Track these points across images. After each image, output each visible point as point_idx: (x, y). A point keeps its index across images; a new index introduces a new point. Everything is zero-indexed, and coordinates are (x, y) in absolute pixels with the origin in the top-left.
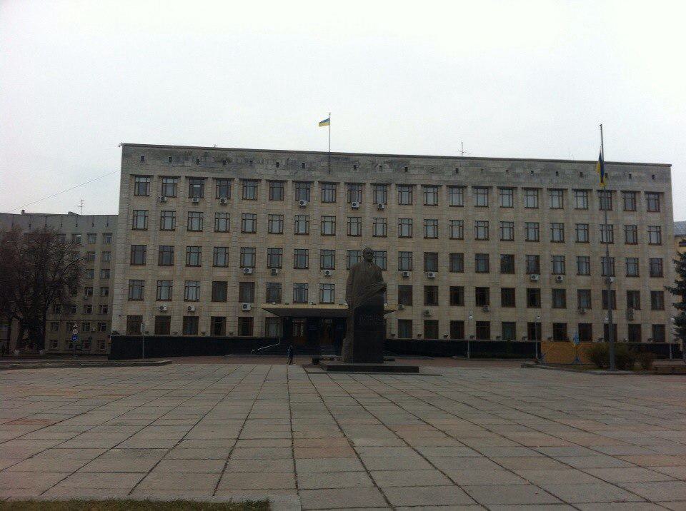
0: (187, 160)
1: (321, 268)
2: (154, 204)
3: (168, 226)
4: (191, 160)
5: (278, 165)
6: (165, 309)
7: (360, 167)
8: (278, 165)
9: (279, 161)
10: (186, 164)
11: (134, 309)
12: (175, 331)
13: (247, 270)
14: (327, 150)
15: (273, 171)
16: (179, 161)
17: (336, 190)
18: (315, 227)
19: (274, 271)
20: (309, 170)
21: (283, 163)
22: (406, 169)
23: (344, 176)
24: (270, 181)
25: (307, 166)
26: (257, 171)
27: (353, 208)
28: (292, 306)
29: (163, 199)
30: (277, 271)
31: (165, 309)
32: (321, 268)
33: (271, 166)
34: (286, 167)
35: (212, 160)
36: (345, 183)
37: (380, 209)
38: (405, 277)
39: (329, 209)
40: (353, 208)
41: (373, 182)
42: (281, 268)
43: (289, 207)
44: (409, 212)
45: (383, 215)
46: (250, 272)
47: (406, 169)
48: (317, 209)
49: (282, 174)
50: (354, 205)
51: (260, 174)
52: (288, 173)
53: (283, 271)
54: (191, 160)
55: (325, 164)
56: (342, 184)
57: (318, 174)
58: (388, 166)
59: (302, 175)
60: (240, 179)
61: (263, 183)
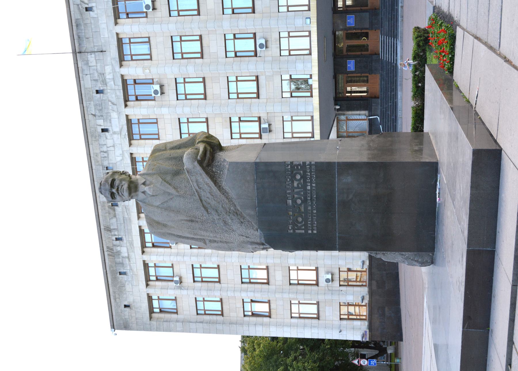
0: (119, 253)
1: (256, 55)
2: (184, 292)
3: (214, 273)
4: (119, 248)
5: (103, 130)
6: (329, 277)
8: (103, 130)
10: (126, 255)
11: (331, 314)
12: (360, 263)
14: (71, 56)
15: (115, 136)
16: (122, 264)
17: (130, 39)
18: (191, 69)
20: (104, 82)
21: (100, 122)
24: (131, 137)
25: (100, 87)
28: (316, 100)
29: (176, 282)
30: (265, 126)
31: (329, 277)
33: (108, 139)
34: (107, 118)
35: (114, 220)
36: (116, 24)
39: (161, 50)
42: (259, 118)
43: (165, 111)
48: (163, 69)
49: (118, 124)
51: (123, 155)
52: (114, 115)
53: (263, 116)
54: (119, 248)
55: (91, 58)
57: (108, 69)
59: (114, 92)
61: (134, 150)
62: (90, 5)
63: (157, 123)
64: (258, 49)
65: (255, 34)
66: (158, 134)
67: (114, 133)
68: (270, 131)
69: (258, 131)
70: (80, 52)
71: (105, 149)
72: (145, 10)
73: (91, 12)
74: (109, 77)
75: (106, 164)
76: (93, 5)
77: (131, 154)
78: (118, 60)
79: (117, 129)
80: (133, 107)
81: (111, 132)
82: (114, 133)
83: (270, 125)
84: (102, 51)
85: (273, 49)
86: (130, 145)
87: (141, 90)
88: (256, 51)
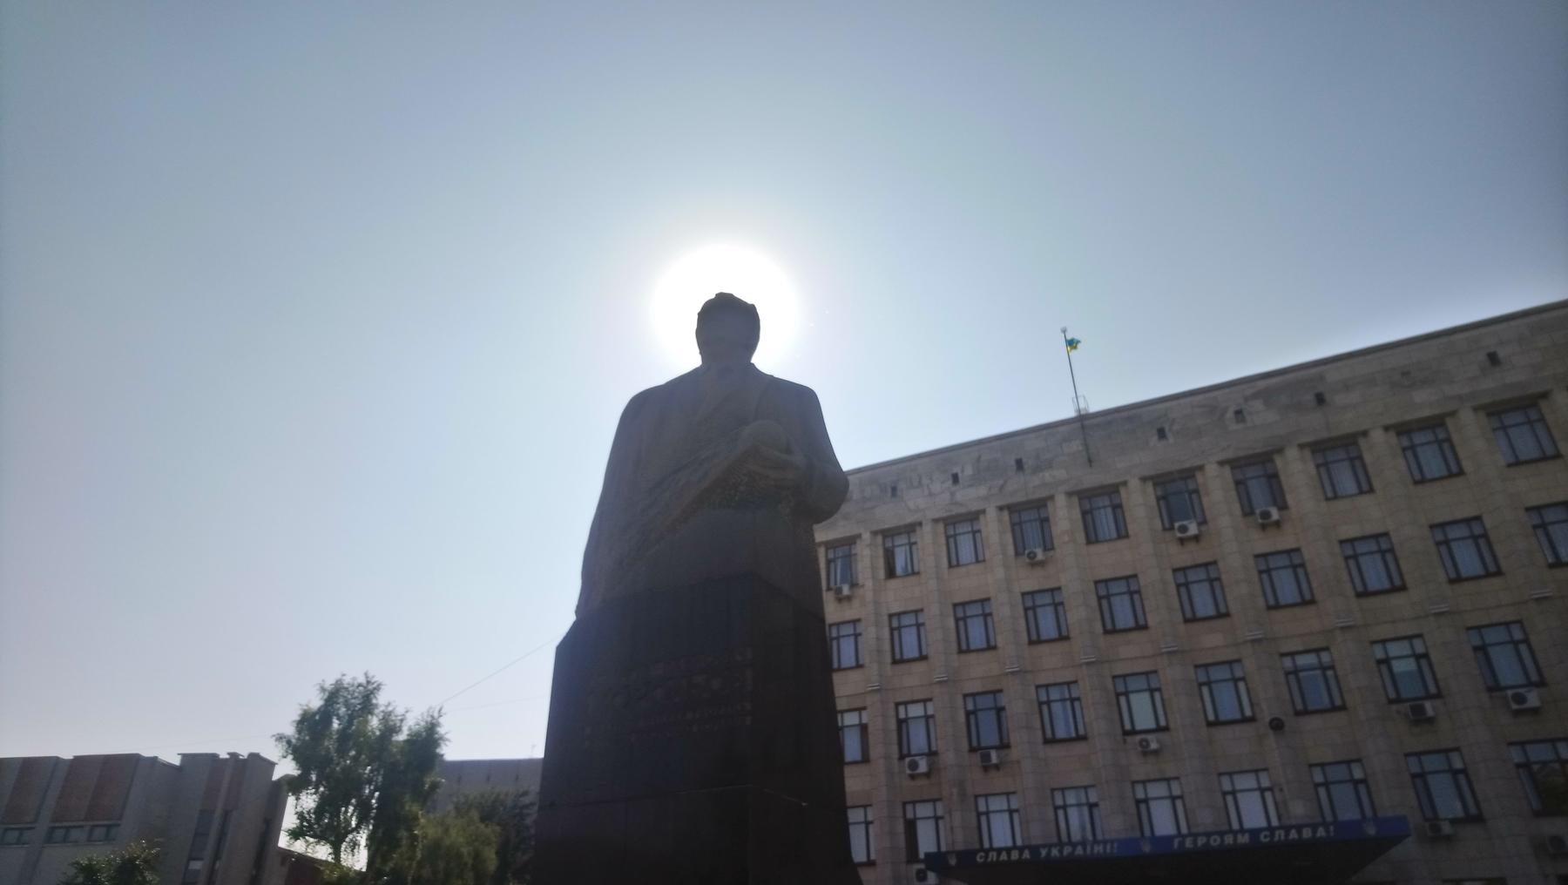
5: (955, 479)
7: (1176, 427)
8: (955, 479)
9: (956, 470)
13: (914, 766)
19: (986, 758)
20: (1037, 469)
21: (969, 471)
22: (1320, 399)
23: (1130, 466)
25: (1029, 463)
26: (911, 505)
27: (1182, 541)
32: (1126, 733)
36: (1144, 479)
37: (1266, 525)
38: (1419, 718)
40: (1182, 541)
41: (1230, 454)
43: (1000, 573)
44: (1369, 514)
45: (1285, 541)
46: (923, 766)
47: (1320, 399)
49: (969, 497)
50: (1184, 529)
55: (1076, 446)
56: (1134, 483)
58: (1258, 405)
60: (875, 533)
61: (927, 528)
62: (1169, 435)
63: (977, 561)
64: (1138, 738)
65: (1166, 729)
66: (958, 565)
67: (953, 494)
68: (986, 769)
69: (983, 744)
70: (1083, 427)
71: (925, 481)
72: (1177, 525)
73: (1155, 438)
74: (1047, 476)
75: (902, 486)
76: (1171, 440)
77: (920, 524)
78: (1079, 488)
79: (959, 497)
80: (1000, 521)
81: (954, 488)
82: (953, 494)
83: (997, 767)
84: (1090, 461)
85: (1141, 769)
86: (936, 521)
87: (1032, 531)
88: (1133, 732)
